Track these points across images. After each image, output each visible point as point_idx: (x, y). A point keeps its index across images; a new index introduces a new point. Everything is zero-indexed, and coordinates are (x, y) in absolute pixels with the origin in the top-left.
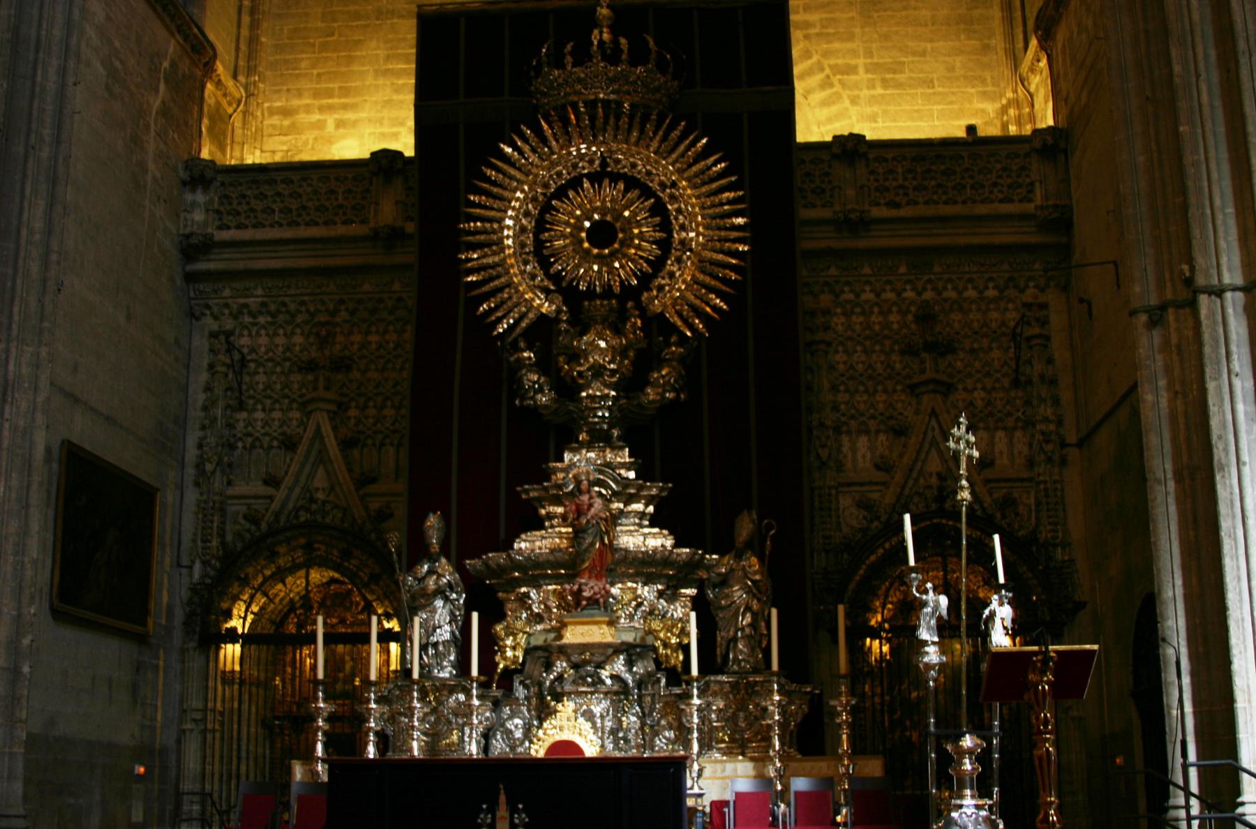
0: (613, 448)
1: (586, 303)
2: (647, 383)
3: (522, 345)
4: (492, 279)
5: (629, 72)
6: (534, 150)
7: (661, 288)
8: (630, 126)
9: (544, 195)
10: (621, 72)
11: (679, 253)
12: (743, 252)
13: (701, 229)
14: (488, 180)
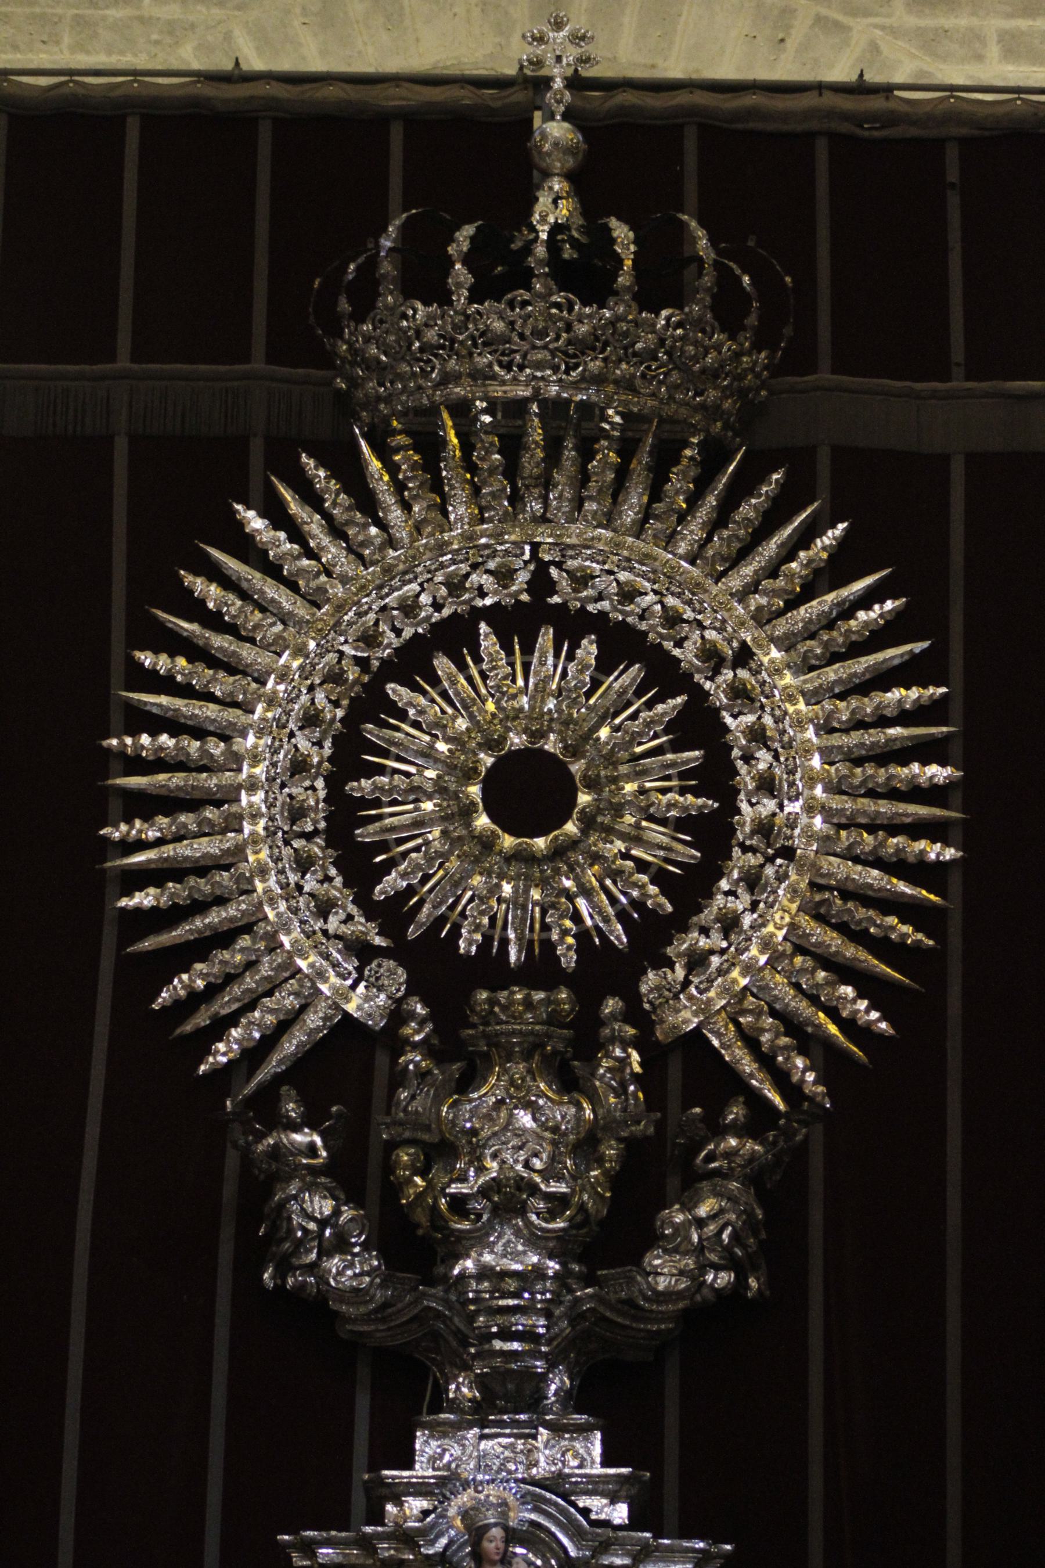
0: (557, 1429)
1: (484, 995)
2: (651, 1239)
3: (292, 1109)
4: (199, 907)
5: (636, 323)
6: (336, 531)
7: (697, 961)
8: (622, 474)
9: (362, 663)
10: (613, 323)
11: (753, 860)
12: (939, 864)
13: (818, 791)
14: (195, 609)
